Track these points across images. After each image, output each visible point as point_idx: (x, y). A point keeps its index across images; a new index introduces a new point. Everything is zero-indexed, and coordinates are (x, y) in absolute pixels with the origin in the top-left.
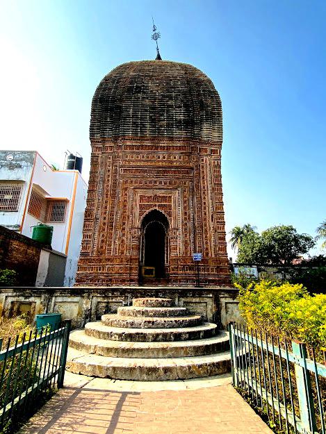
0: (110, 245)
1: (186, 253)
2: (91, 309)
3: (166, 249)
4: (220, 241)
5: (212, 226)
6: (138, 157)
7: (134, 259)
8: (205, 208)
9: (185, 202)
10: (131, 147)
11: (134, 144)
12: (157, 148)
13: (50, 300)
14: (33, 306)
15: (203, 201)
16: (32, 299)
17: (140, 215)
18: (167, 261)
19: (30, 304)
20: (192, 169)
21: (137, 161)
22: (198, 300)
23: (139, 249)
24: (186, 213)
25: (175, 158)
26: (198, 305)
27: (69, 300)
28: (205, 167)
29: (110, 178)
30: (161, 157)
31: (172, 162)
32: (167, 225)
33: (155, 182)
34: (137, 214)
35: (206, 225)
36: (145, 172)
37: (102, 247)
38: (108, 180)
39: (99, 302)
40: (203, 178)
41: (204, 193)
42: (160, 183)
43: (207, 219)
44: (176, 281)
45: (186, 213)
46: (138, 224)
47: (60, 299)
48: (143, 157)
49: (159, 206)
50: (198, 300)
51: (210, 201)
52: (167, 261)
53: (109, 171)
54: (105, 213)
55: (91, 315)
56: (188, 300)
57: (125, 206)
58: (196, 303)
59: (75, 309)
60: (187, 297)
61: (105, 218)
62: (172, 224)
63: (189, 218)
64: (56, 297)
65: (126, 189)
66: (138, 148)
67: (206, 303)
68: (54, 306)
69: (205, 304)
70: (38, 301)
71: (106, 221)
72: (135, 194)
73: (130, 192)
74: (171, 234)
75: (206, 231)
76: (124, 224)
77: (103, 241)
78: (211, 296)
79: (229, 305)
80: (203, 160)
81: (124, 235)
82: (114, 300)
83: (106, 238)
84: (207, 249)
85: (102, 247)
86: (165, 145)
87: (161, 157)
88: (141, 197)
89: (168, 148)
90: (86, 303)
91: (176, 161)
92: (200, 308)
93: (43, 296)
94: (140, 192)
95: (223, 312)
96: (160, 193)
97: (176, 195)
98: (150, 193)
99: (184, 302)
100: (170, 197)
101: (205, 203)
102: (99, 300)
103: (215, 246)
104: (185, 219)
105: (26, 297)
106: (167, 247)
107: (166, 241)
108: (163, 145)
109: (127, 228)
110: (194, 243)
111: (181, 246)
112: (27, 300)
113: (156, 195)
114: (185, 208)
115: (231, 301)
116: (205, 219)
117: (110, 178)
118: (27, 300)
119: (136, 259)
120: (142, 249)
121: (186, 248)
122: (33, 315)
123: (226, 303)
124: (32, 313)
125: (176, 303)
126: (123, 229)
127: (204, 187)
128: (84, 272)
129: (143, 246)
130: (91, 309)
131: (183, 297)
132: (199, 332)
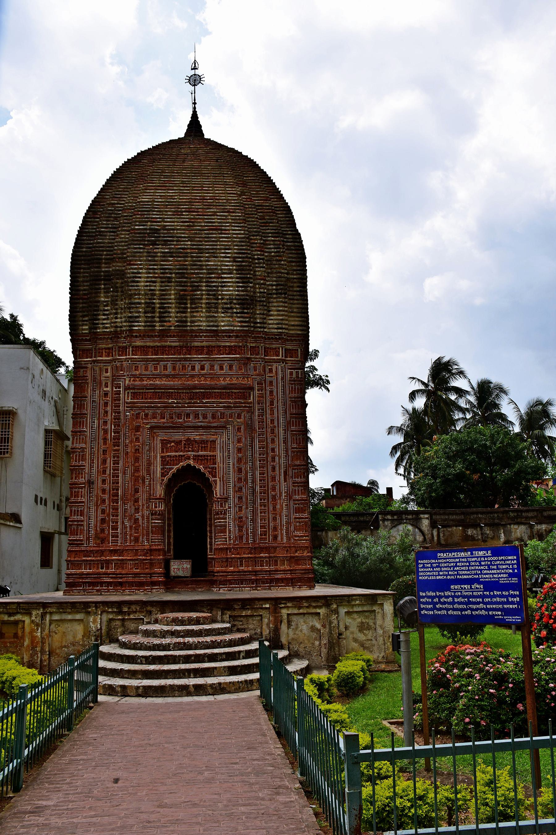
0: (115, 528)
1: (241, 538)
2: (101, 628)
3: (208, 529)
4: (297, 515)
5: (284, 489)
6: (156, 369)
7: (156, 550)
8: (273, 460)
9: (239, 450)
10: (144, 350)
11: (148, 344)
12: (190, 350)
13: (43, 616)
14: (20, 626)
15: (271, 446)
16: (19, 617)
17: (163, 475)
18: (211, 549)
19: (16, 623)
20: (252, 388)
21: (160, 376)
22: (249, 613)
23: (164, 531)
24: (240, 470)
25: (221, 368)
26: (250, 620)
27: (70, 617)
28: (274, 383)
29: (109, 409)
30: (197, 367)
31: (213, 377)
32: (209, 487)
33: (188, 415)
34: (159, 474)
35: (274, 489)
36: (170, 396)
37: (103, 530)
38: (106, 412)
39: (111, 620)
40: (272, 403)
41: (273, 432)
42: (196, 416)
43: (277, 478)
44: (224, 583)
45: (240, 470)
46: (160, 491)
47: (56, 617)
48: (165, 368)
49: (196, 458)
50: (249, 613)
51: (282, 445)
52: (211, 549)
53: (106, 395)
54: (104, 472)
55: (101, 637)
56: (236, 613)
57: (137, 459)
58: (246, 616)
59: (79, 629)
60: (234, 610)
61: (104, 481)
62: (218, 491)
63: (246, 480)
64: (51, 613)
65: (137, 429)
66: (156, 350)
67: (261, 615)
68: (50, 625)
69: (259, 618)
70: (27, 619)
71: (106, 486)
72: (153, 437)
73: (145, 434)
74: (216, 507)
75: (274, 497)
76: (137, 491)
77: (103, 521)
78: (268, 606)
79: (294, 618)
80: (271, 371)
81: (137, 510)
82: (132, 617)
83: (108, 515)
84: (275, 529)
85: (103, 530)
86: (205, 344)
87: (197, 367)
88: (164, 443)
89: (210, 350)
90: (95, 621)
91: (225, 376)
92: (253, 624)
93: (34, 613)
94: (162, 435)
95: (284, 627)
96: (195, 436)
97: (221, 439)
98: (178, 436)
99: (230, 616)
100: (214, 442)
101: (273, 450)
102: (111, 616)
103: (288, 523)
104: (240, 480)
105: (10, 615)
106: (211, 527)
107: (208, 516)
108: (199, 344)
109: (142, 496)
110: (253, 520)
111: (231, 526)
112: (12, 619)
113: (188, 439)
114: (239, 460)
115: (296, 611)
116: (273, 479)
117: (109, 409)
118: (12, 619)
119: (159, 550)
120: (169, 531)
121: (240, 530)
122: (23, 637)
123: (288, 614)
124: (20, 633)
125: (219, 618)
126: (136, 501)
127: (272, 421)
128: (79, 571)
129: (169, 525)
130: (101, 628)
131: (228, 610)
132: (240, 652)
